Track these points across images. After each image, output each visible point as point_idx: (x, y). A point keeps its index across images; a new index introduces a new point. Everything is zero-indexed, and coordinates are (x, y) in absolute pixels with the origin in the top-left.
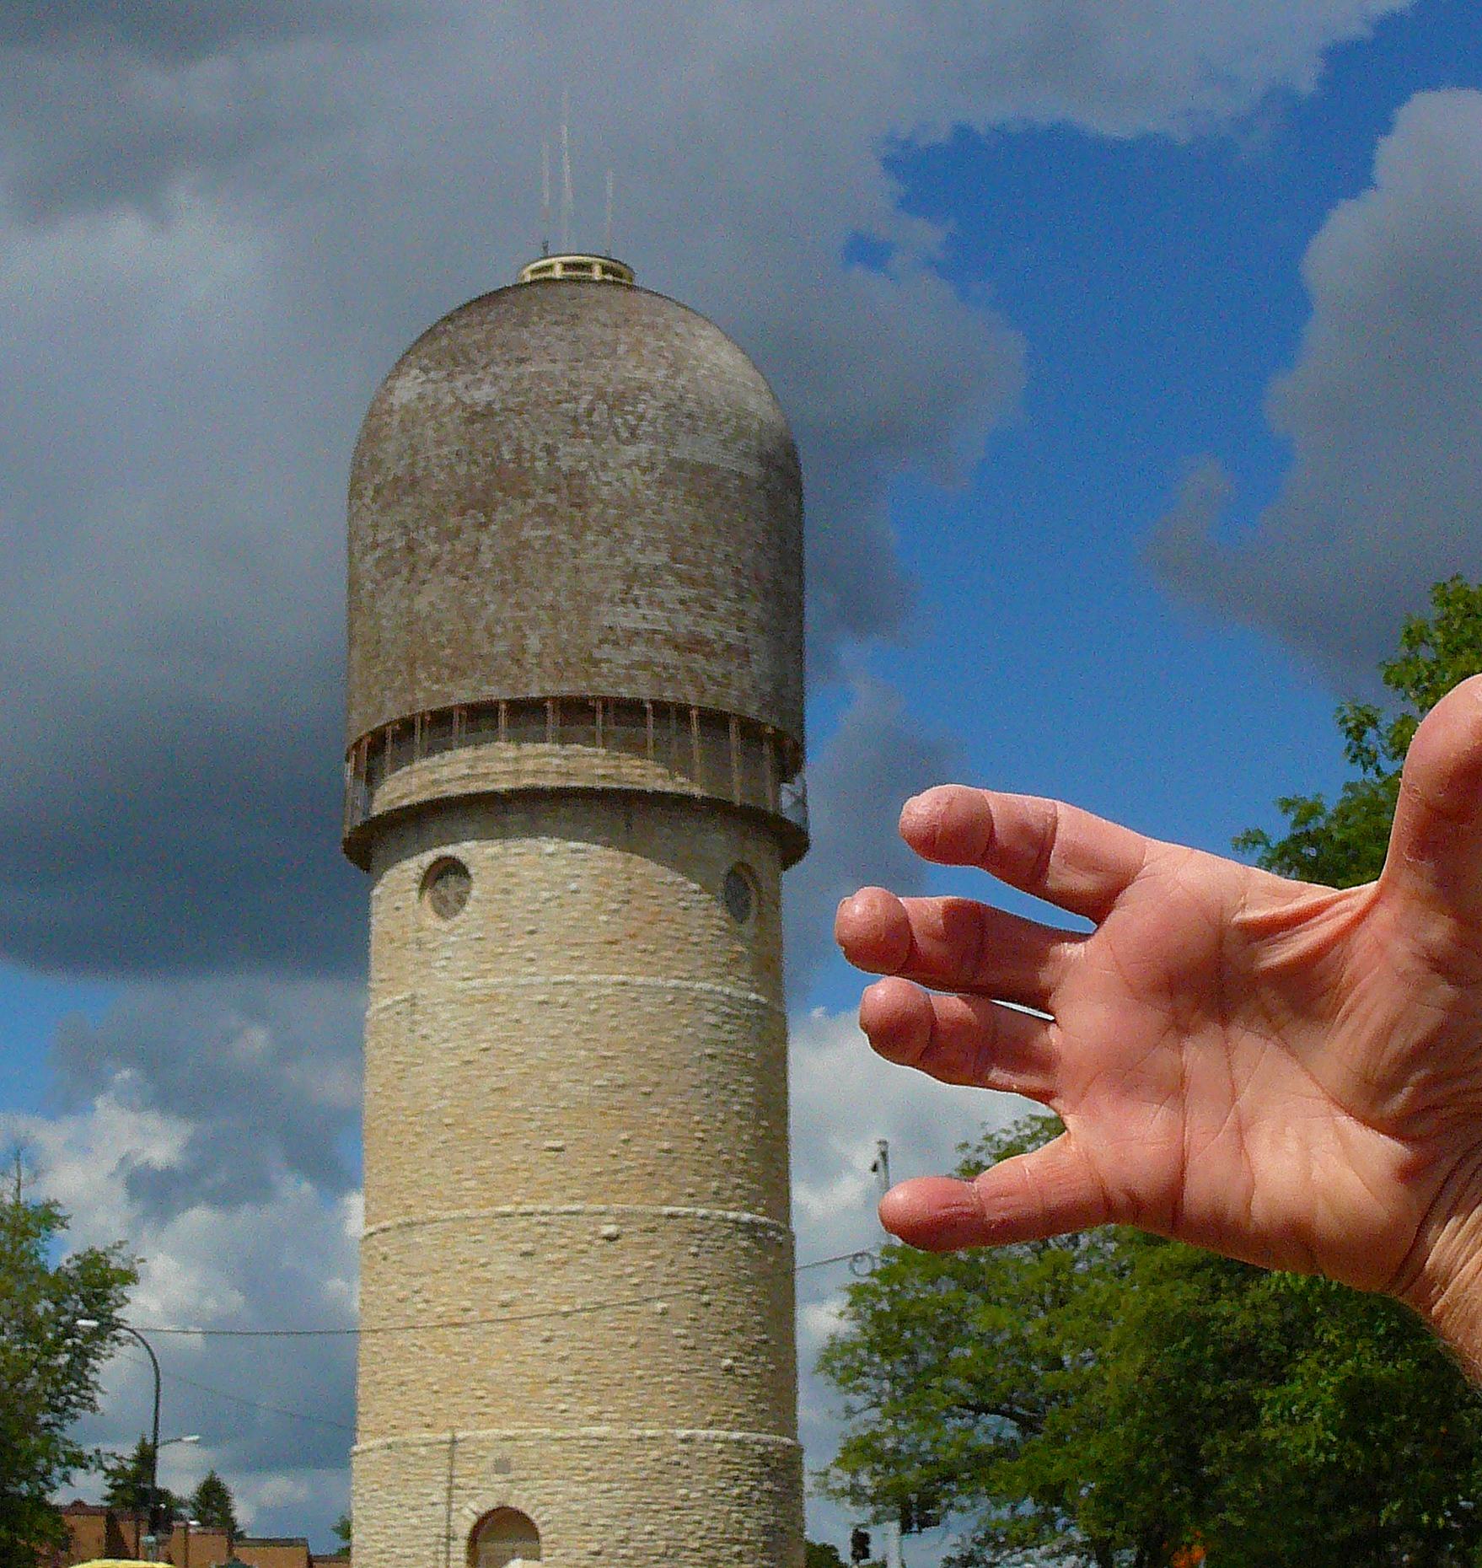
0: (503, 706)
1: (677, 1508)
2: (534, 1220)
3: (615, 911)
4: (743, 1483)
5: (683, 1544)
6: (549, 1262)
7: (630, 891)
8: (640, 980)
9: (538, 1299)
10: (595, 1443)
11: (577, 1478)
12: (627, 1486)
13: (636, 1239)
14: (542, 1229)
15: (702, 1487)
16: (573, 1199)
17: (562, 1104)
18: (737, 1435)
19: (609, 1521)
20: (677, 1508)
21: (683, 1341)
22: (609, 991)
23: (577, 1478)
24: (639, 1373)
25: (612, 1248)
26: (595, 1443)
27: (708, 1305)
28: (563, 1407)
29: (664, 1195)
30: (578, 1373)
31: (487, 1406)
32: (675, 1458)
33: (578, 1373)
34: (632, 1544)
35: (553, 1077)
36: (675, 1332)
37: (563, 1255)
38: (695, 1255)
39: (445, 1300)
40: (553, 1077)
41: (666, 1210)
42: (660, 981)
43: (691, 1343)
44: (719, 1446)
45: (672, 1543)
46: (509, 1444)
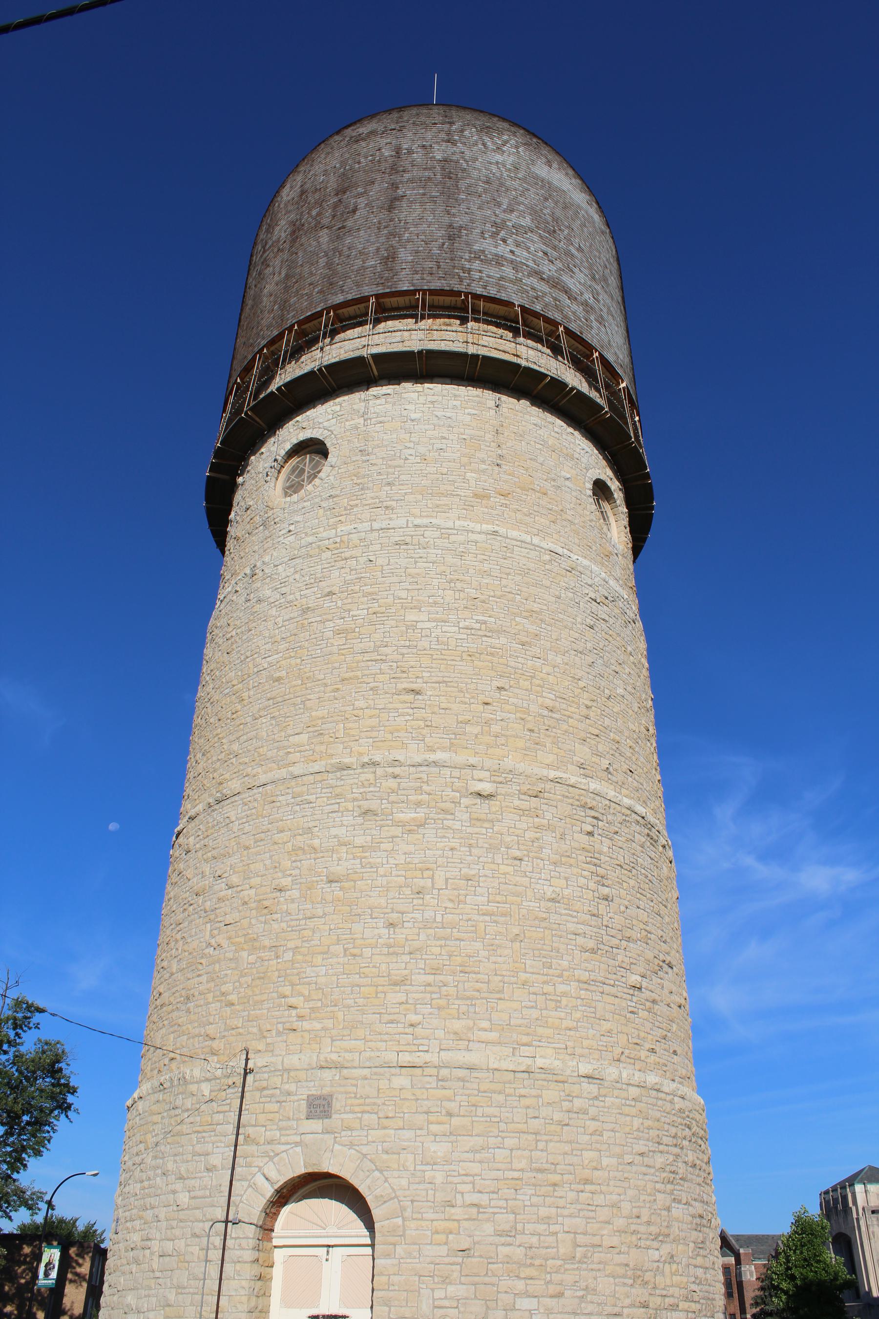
0: (372, 300)
1: (587, 1181)
2: (380, 771)
3: (484, 471)
4: (666, 1148)
5: (596, 1240)
6: (402, 824)
7: (501, 456)
8: (514, 534)
9: (381, 871)
10: (461, 1073)
11: (434, 1128)
12: (509, 1142)
13: (517, 803)
14: (392, 783)
15: (617, 1150)
16: (431, 750)
17: (425, 643)
18: (652, 1079)
19: (484, 1199)
20: (587, 1181)
21: (580, 940)
22: (481, 538)
23: (434, 1128)
24: (523, 976)
25: (482, 808)
26: (461, 1073)
27: (606, 898)
28: (413, 1018)
29: (551, 759)
30: (435, 971)
31: (301, 1017)
32: (578, 1103)
33: (435, 971)
34: (520, 1239)
35: (411, 616)
36: (571, 927)
37: (420, 815)
38: (590, 834)
39: (256, 881)
40: (411, 616)
41: (552, 774)
42: (536, 540)
43: (591, 944)
44: (634, 1092)
45: (581, 1239)
46: (327, 1074)
